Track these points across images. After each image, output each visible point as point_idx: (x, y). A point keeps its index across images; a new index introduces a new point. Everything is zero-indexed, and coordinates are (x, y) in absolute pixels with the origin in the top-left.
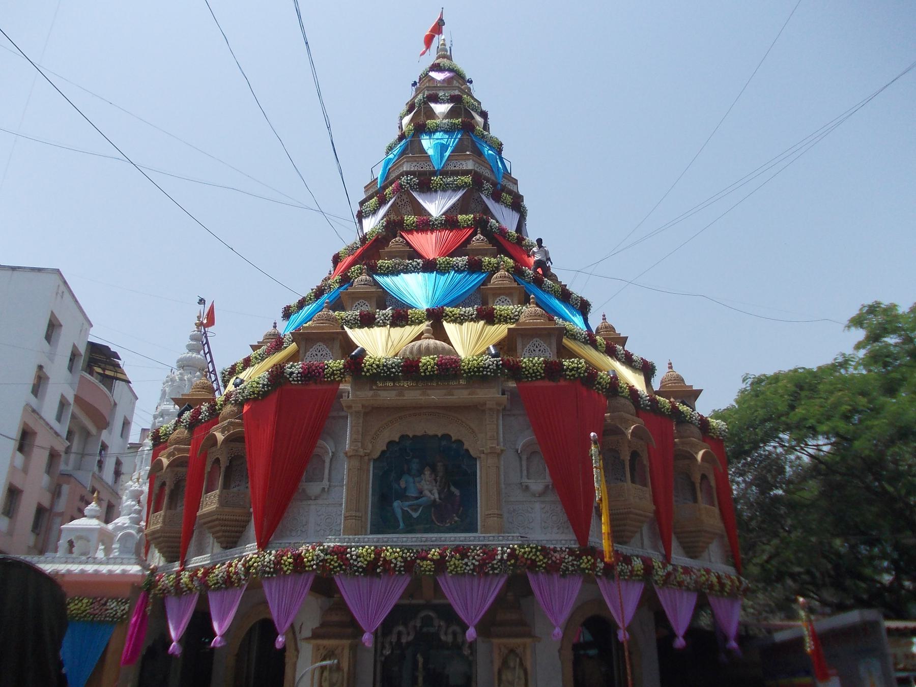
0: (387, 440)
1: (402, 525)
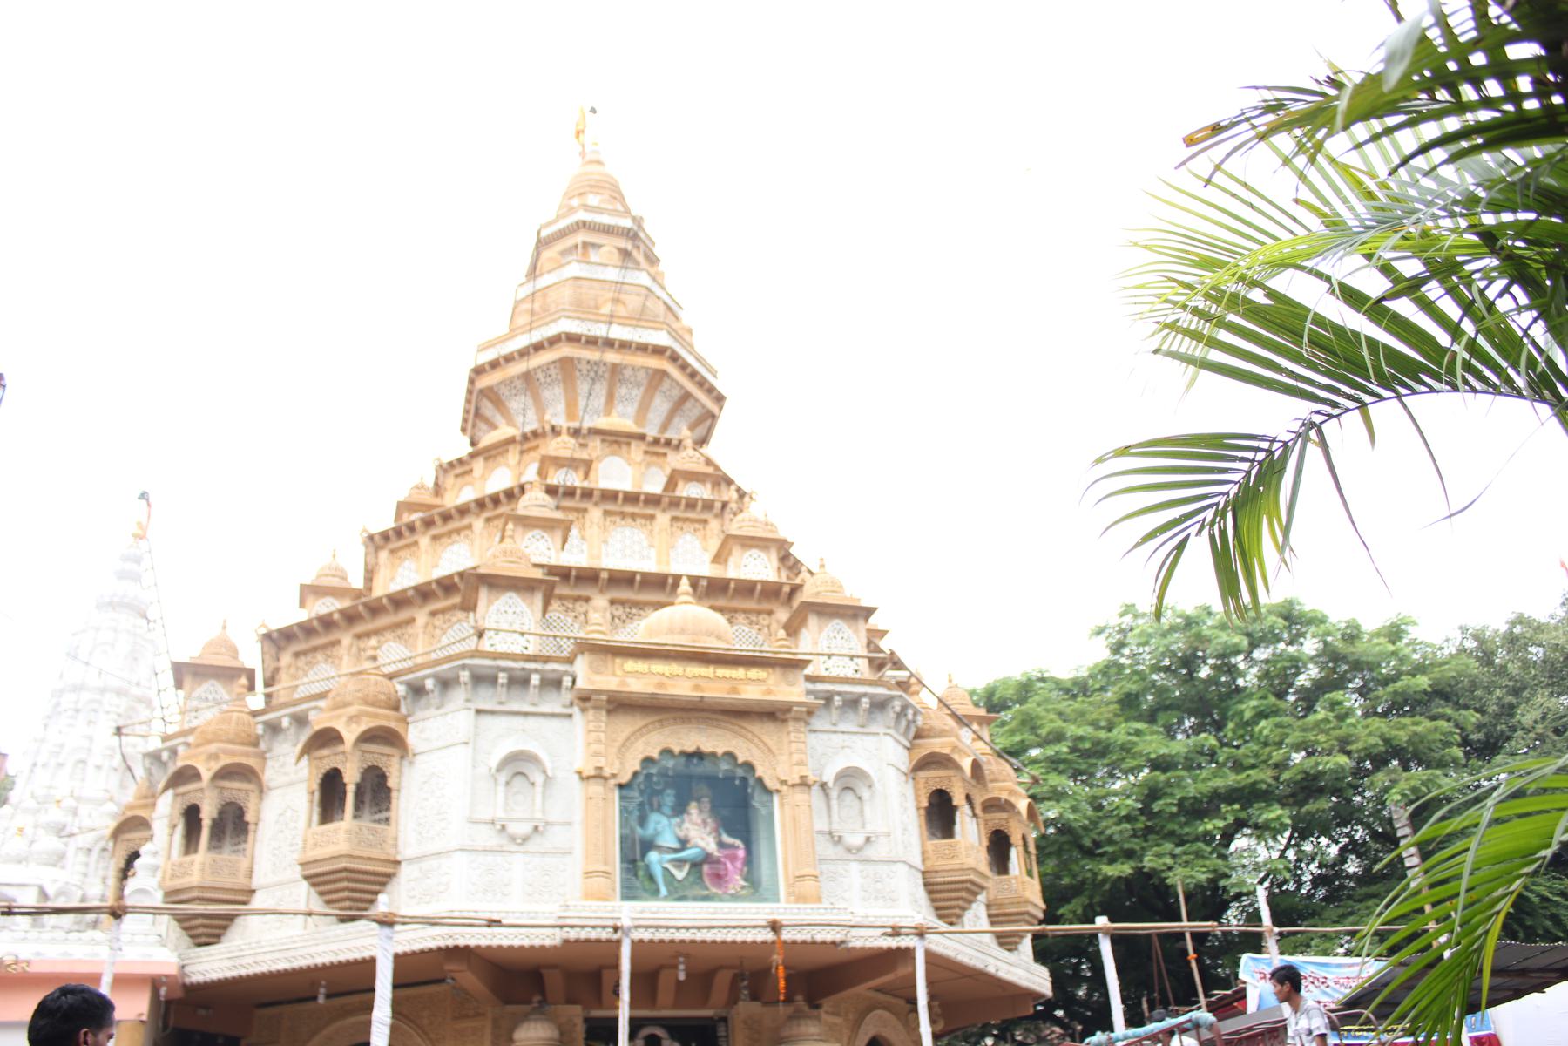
0: (640, 757)
1: (663, 891)
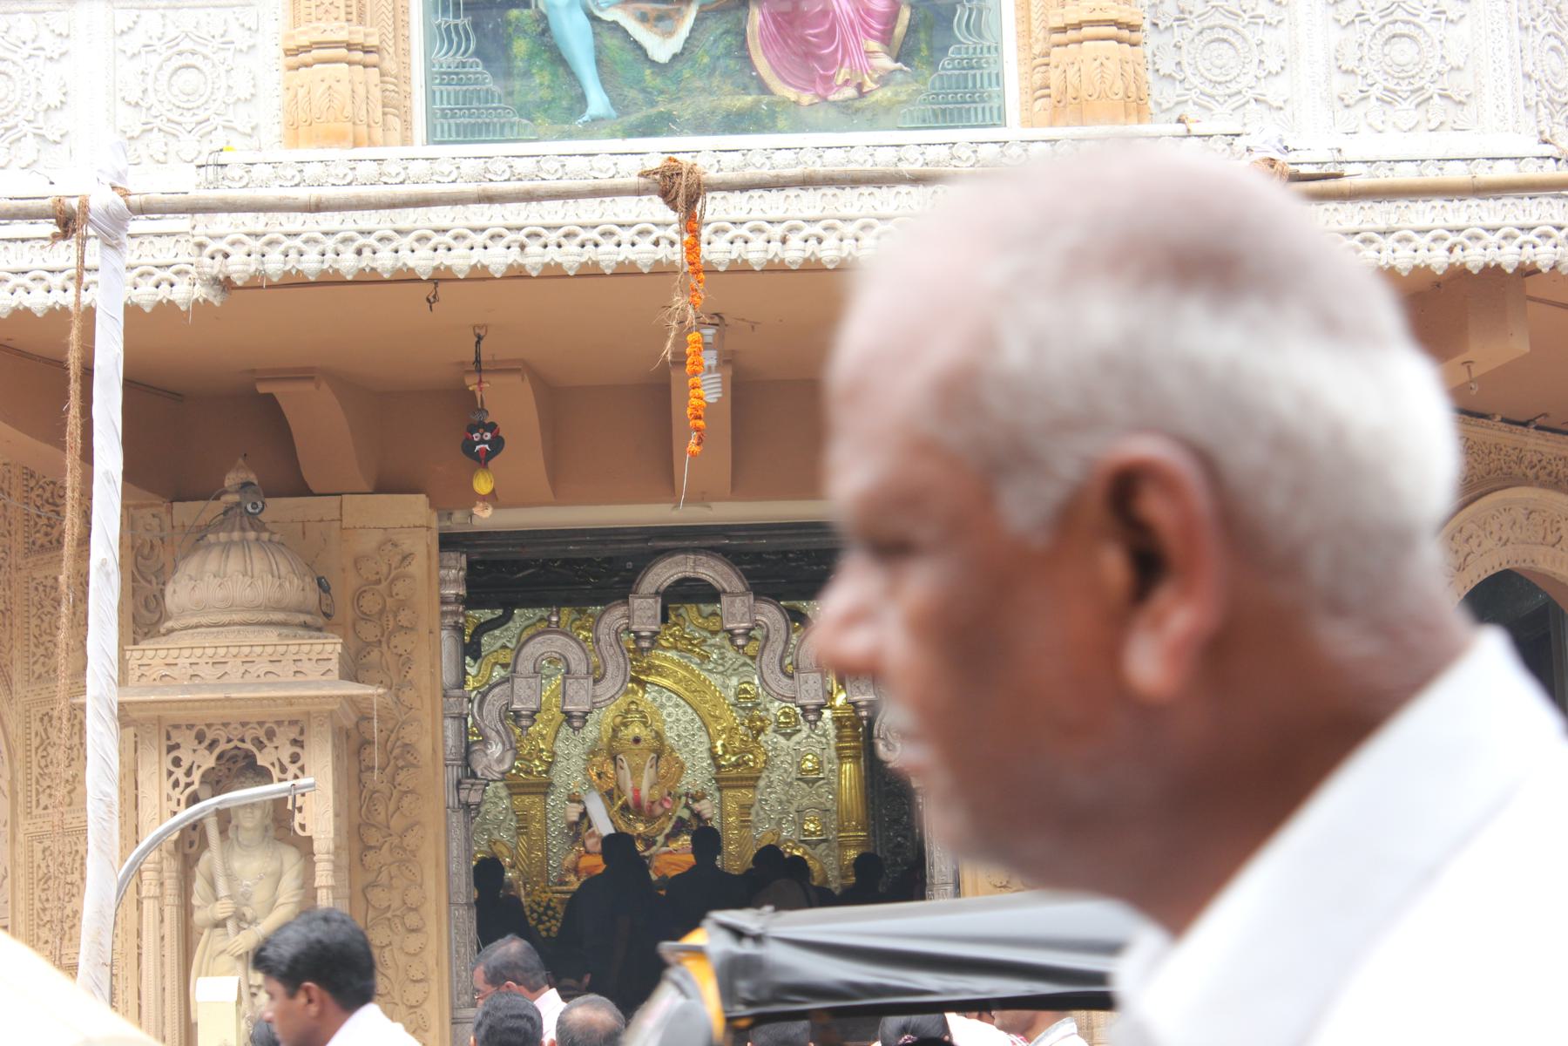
1: (598, 101)
